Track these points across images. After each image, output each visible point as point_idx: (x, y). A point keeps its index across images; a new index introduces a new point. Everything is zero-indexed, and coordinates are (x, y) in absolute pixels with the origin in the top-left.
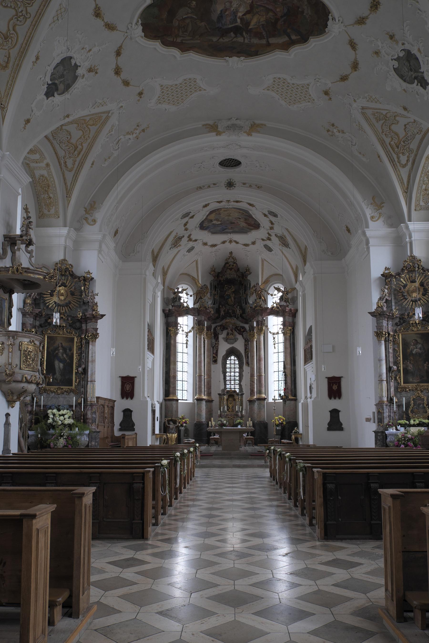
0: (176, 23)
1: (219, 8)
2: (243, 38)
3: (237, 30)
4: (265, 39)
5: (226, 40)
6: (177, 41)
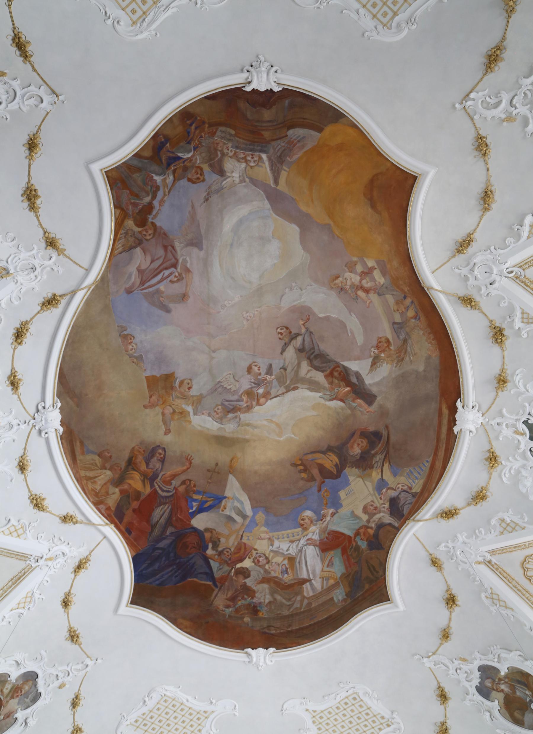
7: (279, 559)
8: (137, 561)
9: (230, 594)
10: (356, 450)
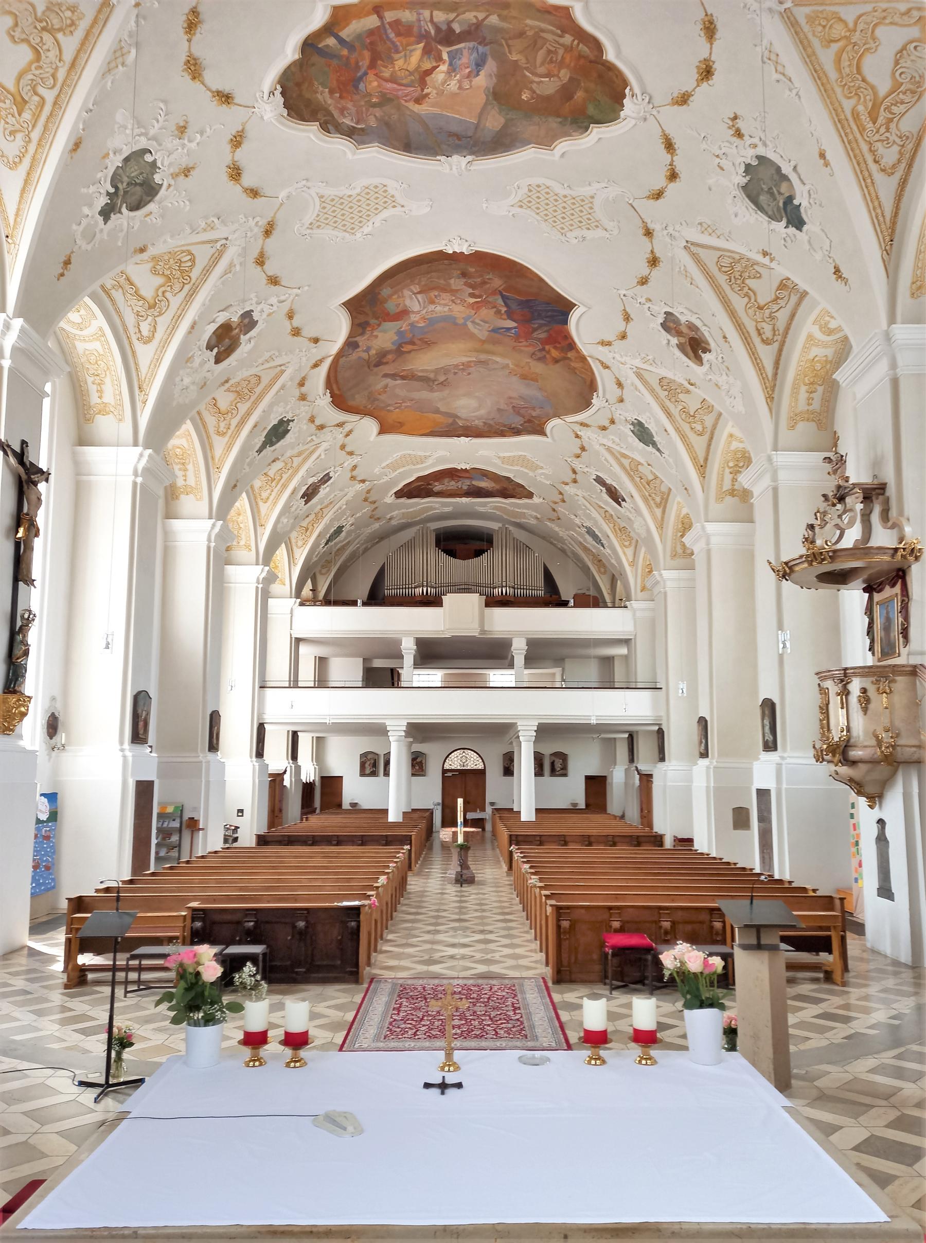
0: (565, 75)
1: (482, 80)
2: (435, 20)
3: (448, 37)
4: (389, 23)
5: (470, 16)
6: (571, 38)
7: (443, 302)
8: (565, 322)
9: (488, 286)
10: (390, 357)
